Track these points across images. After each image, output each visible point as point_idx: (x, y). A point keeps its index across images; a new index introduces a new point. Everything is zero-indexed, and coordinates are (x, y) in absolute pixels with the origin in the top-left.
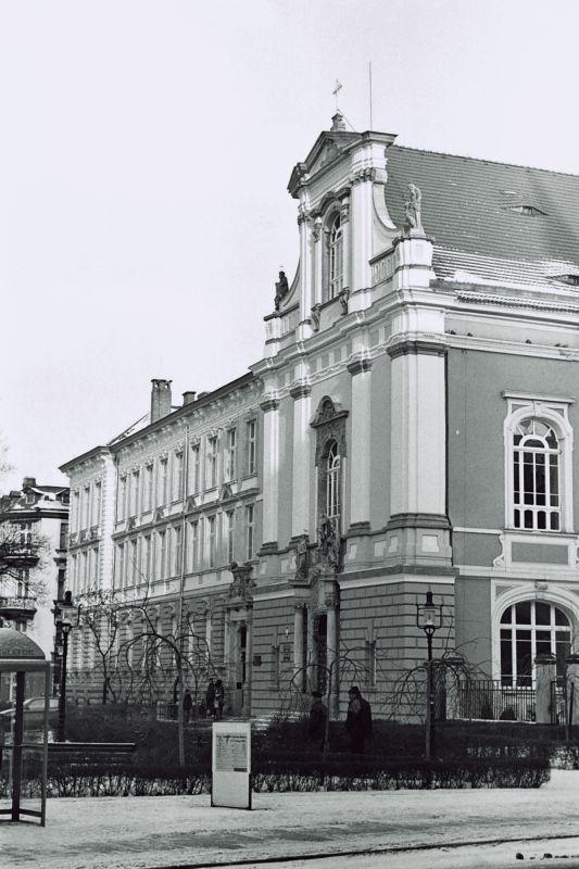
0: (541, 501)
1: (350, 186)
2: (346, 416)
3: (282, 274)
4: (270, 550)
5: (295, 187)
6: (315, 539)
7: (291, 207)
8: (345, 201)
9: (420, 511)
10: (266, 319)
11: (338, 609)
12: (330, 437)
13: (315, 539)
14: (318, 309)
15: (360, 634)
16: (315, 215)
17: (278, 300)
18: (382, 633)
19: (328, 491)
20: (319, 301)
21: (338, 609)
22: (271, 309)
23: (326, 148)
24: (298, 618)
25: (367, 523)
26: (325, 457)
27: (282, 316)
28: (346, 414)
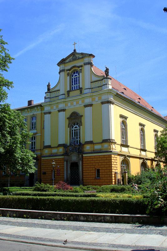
0: (124, 139)
1: (83, 65)
2: (82, 117)
3: (49, 83)
4: (49, 147)
5: (59, 64)
6: (68, 144)
7: (58, 69)
8: (81, 68)
9: (113, 139)
10: (46, 93)
11: (82, 161)
12: (75, 121)
13: (68, 144)
14: (68, 92)
15: (93, 166)
16: (69, 70)
17: (49, 89)
18: (101, 166)
19: (75, 135)
20: (68, 89)
21: (82, 161)
22: (46, 91)
23: (72, 56)
24: (65, 163)
25: (92, 141)
26: (71, 126)
27: (51, 92)
28: (82, 116)
